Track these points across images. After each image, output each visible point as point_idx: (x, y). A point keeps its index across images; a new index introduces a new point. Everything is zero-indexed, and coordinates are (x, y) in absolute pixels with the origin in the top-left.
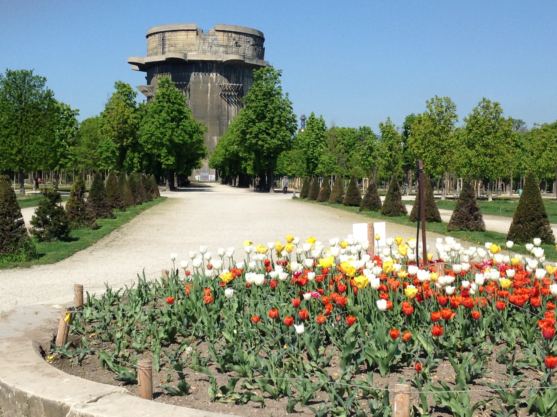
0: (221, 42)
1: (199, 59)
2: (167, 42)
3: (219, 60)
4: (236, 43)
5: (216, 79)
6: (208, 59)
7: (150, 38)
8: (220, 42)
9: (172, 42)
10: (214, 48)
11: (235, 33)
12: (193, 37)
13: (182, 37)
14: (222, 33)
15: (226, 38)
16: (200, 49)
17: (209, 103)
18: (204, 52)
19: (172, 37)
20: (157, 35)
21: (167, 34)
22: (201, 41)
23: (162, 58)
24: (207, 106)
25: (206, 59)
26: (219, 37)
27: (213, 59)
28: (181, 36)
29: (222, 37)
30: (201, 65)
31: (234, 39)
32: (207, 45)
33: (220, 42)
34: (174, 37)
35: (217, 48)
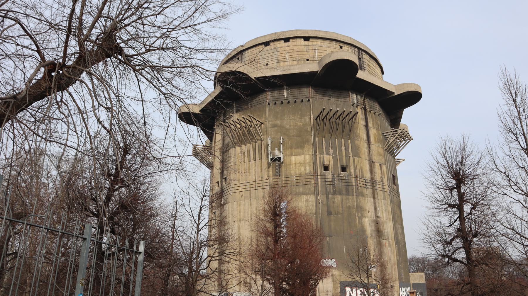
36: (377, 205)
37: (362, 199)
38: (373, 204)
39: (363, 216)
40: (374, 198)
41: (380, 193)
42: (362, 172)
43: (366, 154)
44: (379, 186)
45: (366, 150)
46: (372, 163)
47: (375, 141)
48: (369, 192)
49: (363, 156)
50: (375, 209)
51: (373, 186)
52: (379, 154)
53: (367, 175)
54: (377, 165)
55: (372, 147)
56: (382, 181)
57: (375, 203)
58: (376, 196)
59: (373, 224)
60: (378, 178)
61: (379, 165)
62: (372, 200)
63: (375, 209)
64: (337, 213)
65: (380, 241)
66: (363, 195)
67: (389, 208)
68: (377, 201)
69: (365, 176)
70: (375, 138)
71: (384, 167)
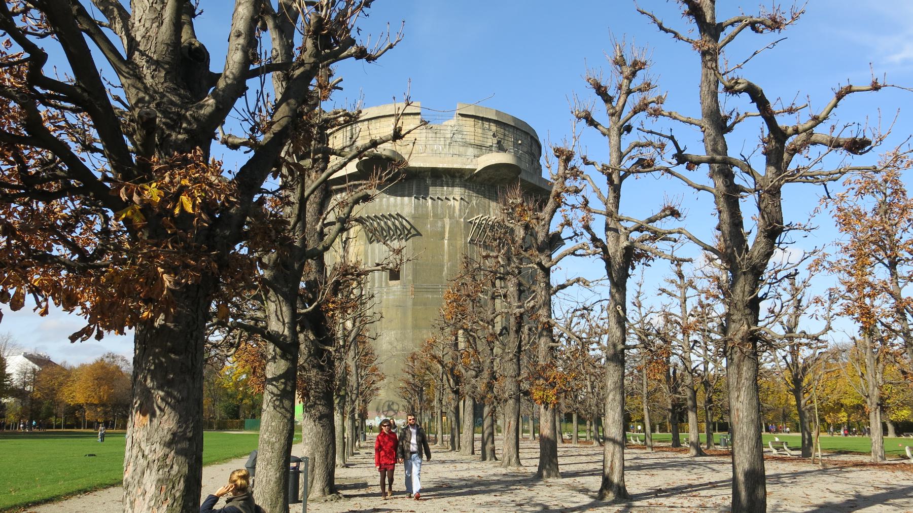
0: (470, 139)
3: (467, 167)
4: (499, 142)
5: (460, 210)
6: (446, 166)
8: (468, 137)
10: (456, 149)
11: (496, 122)
14: (471, 121)
15: (480, 131)
16: (428, 150)
17: (446, 257)
18: (435, 153)
22: (430, 135)
24: (443, 266)
25: (441, 166)
26: (465, 129)
27: (455, 166)
29: (472, 129)
31: (494, 136)
32: (442, 143)
33: (468, 137)
35: (462, 149)
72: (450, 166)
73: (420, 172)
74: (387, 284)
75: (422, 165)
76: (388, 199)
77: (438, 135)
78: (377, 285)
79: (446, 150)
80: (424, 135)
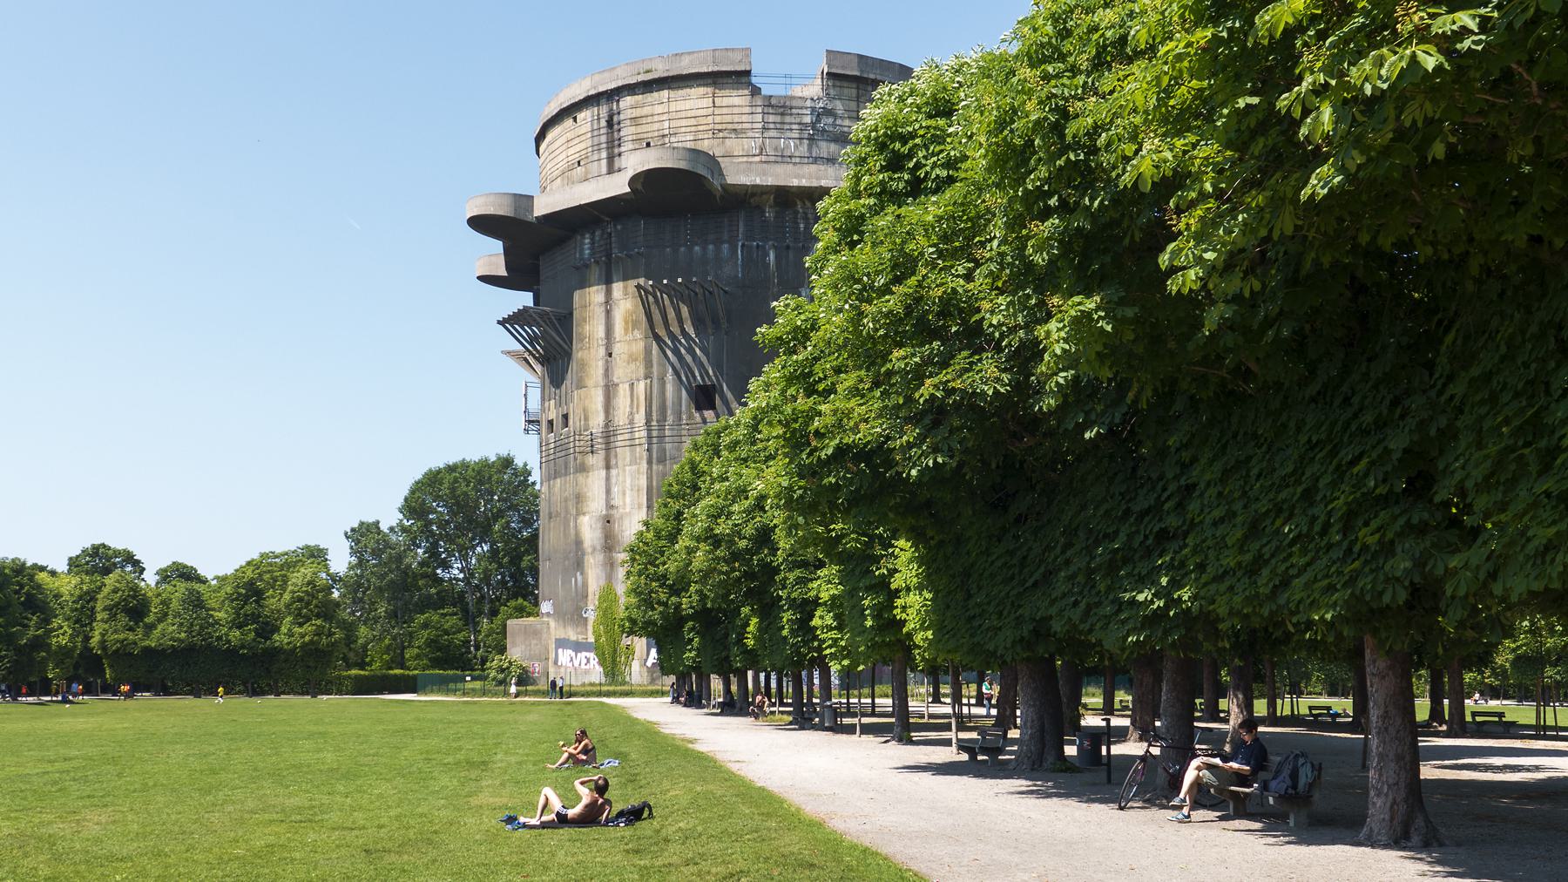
1: (770, 181)
2: (627, 131)
6: (804, 183)
7: (550, 136)
9: (650, 129)
12: (737, 101)
13: (688, 105)
18: (783, 158)
19: (646, 110)
20: (584, 116)
21: (627, 101)
22: (771, 118)
23: (618, 186)
25: (795, 183)
28: (695, 100)
30: (769, 214)
34: (659, 109)
35: (833, 147)
36: (613, 480)
37: (581, 478)
38: (603, 483)
39: (580, 513)
40: (608, 467)
41: (623, 454)
42: (586, 419)
43: (601, 371)
44: (621, 439)
45: (601, 364)
46: (609, 391)
47: (626, 330)
48: (596, 460)
49: (590, 382)
50: (608, 491)
51: (608, 443)
52: (632, 359)
53: (597, 422)
54: (623, 390)
55: (618, 349)
56: (631, 422)
57: (608, 479)
58: (613, 462)
59: (599, 525)
60: (621, 418)
61: (627, 386)
62: (603, 473)
63: (608, 491)
64: (558, 515)
65: (611, 558)
66: (583, 469)
67: (643, 482)
68: (614, 472)
69: (591, 423)
70: (626, 323)
71: (641, 387)
72: (815, 184)
73: (753, 195)
74: (690, 417)
75: (758, 182)
76: (690, 249)
77: (788, 119)
78: (670, 419)
79: (804, 149)
80: (759, 118)
